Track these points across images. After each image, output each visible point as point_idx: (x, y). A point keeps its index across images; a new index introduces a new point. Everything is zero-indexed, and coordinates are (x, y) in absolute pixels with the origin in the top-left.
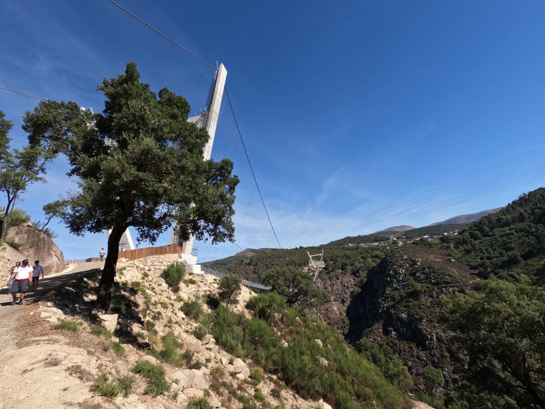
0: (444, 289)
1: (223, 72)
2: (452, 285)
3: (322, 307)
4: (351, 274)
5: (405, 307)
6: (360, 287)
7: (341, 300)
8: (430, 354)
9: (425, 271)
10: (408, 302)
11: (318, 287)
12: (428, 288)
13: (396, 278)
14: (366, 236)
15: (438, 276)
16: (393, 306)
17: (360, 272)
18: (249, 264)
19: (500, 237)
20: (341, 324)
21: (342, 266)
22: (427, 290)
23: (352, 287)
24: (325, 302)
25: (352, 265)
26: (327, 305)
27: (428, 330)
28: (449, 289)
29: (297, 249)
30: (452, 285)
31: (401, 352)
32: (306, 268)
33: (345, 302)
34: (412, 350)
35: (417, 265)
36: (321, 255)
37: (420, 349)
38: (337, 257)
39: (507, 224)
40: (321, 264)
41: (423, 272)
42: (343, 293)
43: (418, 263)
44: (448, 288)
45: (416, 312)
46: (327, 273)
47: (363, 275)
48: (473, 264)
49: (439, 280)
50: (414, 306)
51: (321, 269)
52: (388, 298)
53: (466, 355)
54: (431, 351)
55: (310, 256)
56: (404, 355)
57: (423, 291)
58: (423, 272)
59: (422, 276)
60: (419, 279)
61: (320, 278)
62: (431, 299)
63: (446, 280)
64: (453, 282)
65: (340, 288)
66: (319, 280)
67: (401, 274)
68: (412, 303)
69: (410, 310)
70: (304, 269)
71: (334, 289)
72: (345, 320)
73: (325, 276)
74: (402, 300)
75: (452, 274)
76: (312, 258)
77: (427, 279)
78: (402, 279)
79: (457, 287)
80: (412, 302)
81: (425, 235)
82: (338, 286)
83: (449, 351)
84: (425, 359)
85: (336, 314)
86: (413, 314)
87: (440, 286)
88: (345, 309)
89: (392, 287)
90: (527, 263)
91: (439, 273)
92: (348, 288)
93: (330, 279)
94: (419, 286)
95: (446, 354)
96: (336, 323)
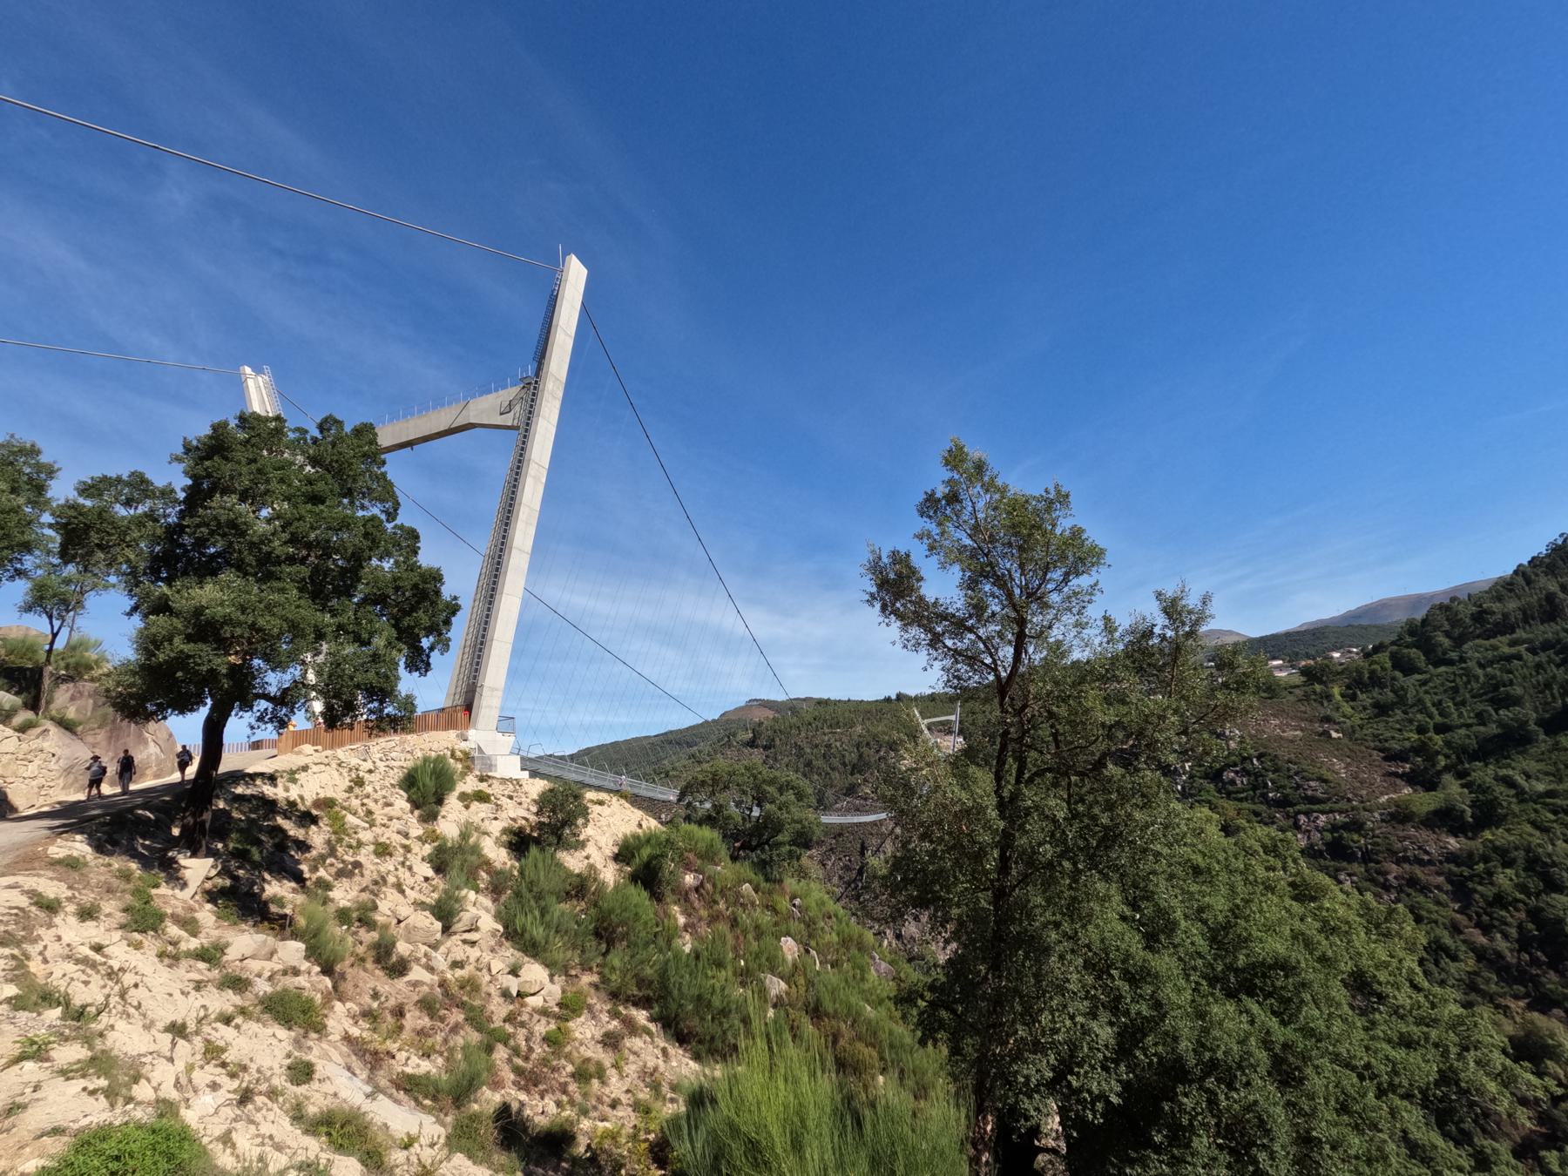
0: (1302, 818)
1: (576, 275)
2: (1327, 807)
9: (1249, 767)
18: (752, 744)
19: (1481, 666)
28: (1317, 818)
29: (888, 700)
30: (1327, 807)
36: (952, 718)
39: (1504, 627)
41: (1244, 769)
44: (1315, 814)
48: (1396, 746)
49: (1288, 791)
55: (923, 724)
58: (1244, 769)
60: (1230, 788)
63: (1309, 793)
64: (1329, 799)
75: (1328, 776)
77: (1254, 788)
78: (1183, 788)
79: (1340, 812)
81: (1274, 658)
87: (1291, 810)
90: (1557, 743)
91: (1292, 773)
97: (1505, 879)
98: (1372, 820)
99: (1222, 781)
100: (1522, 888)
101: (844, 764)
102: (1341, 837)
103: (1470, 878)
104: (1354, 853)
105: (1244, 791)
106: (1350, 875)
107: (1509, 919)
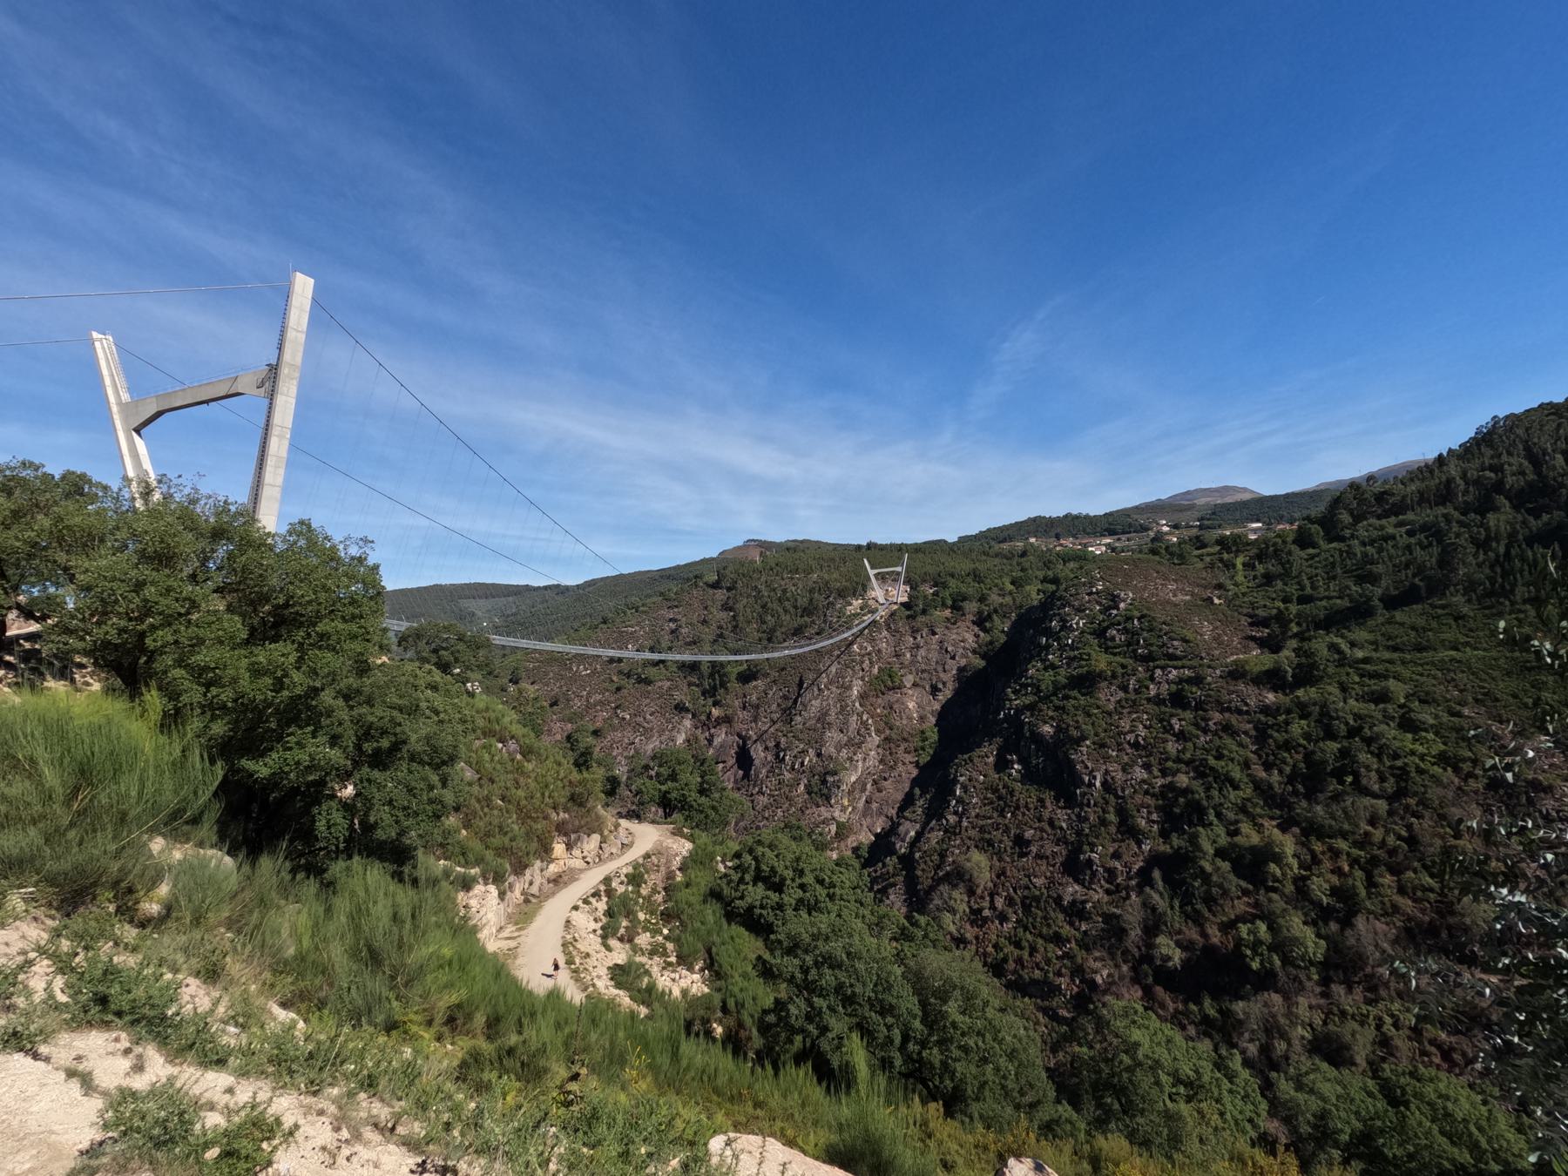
0: (1158, 672)
1: (303, 287)
3: (880, 701)
4: (974, 623)
5: (1057, 708)
6: (983, 657)
7: (932, 686)
8: (1078, 816)
9: (1129, 626)
10: (1066, 697)
11: (879, 651)
12: (1123, 666)
13: (1058, 639)
14: (1087, 517)
15: (1154, 641)
16: (1031, 707)
17: (995, 617)
18: (715, 586)
19: (1364, 544)
20: (917, 742)
21: (954, 601)
22: (1120, 670)
23: (963, 656)
24: (889, 689)
25: (982, 599)
26: (893, 697)
27: (1089, 765)
30: (1180, 663)
31: (1017, 808)
32: (857, 603)
33: (940, 690)
34: (1044, 807)
35: (1118, 609)
36: (899, 569)
37: (1062, 804)
38: (952, 576)
40: (901, 594)
42: (940, 669)
43: (1122, 605)
45: (1077, 722)
46: (908, 617)
47: (1002, 626)
48: (1261, 613)
49: (1154, 648)
50: (1076, 709)
51: (895, 607)
52: (1025, 686)
53: (1153, 822)
54: (1082, 809)
55: (872, 572)
56: (1024, 814)
57: (1109, 673)
58: (1125, 628)
59: (1120, 638)
60: (1110, 643)
61: (889, 629)
62: (1121, 694)
63: (1171, 651)
64: (1185, 657)
65: (934, 656)
66: (885, 633)
67: (1074, 630)
68: (1073, 702)
69: (1065, 717)
70: (851, 604)
71: (919, 658)
72: (928, 734)
73: (903, 626)
74: (1055, 694)
75: (1190, 636)
76: (876, 576)
79: (1189, 668)
80: (1075, 698)
81: (1252, 522)
82: (929, 652)
83: (1122, 812)
84: (1064, 825)
85: (910, 718)
86: (1068, 726)
88: (937, 706)
89: (1043, 661)
90: (1393, 617)
92: (953, 658)
93: (914, 631)
94: (1101, 662)
95: (1112, 817)
96: (905, 740)
97: (1298, 728)
98: (1212, 676)
99: (1105, 638)
100: (1307, 736)
101: (796, 607)
102: (1182, 689)
103: (1271, 727)
104: (1189, 702)
105: (1119, 646)
106: (1180, 720)
107: (1289, 760)
